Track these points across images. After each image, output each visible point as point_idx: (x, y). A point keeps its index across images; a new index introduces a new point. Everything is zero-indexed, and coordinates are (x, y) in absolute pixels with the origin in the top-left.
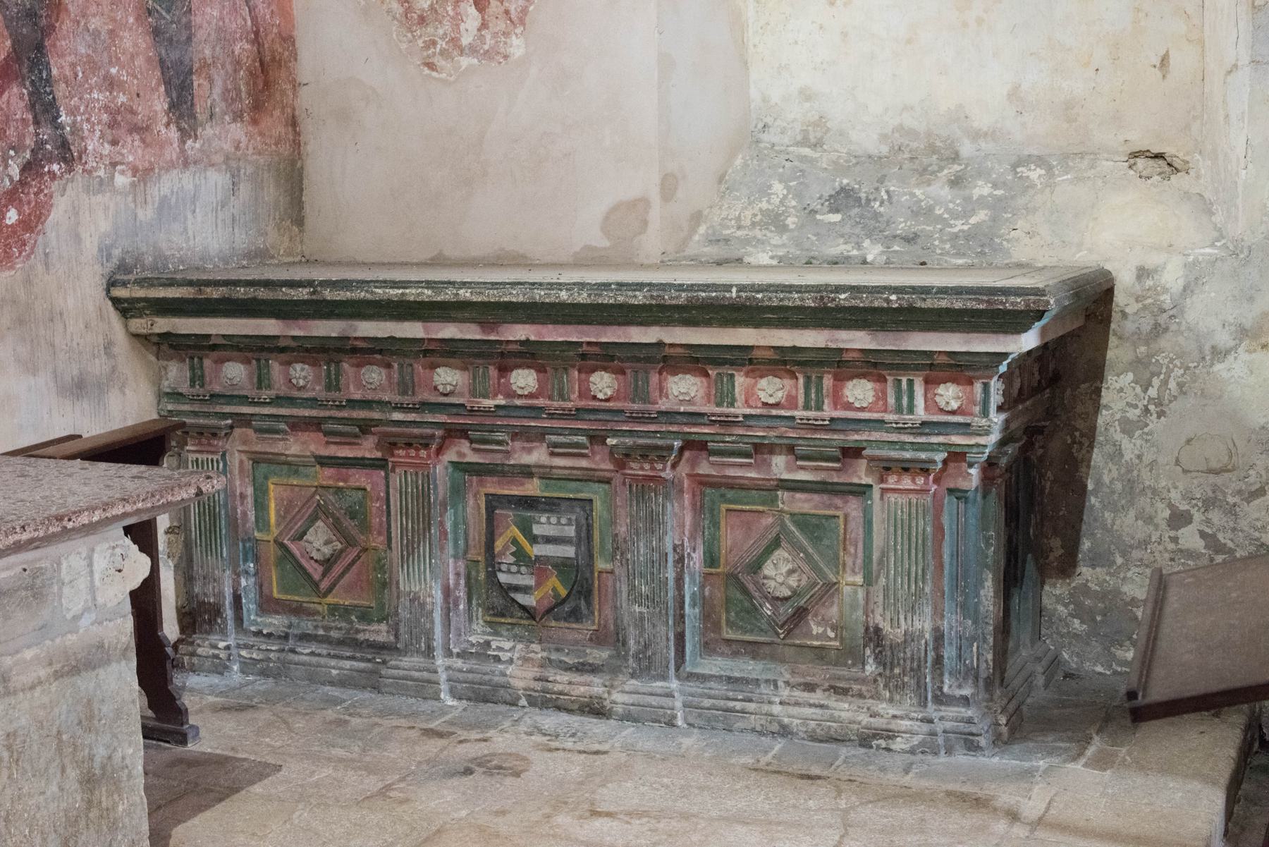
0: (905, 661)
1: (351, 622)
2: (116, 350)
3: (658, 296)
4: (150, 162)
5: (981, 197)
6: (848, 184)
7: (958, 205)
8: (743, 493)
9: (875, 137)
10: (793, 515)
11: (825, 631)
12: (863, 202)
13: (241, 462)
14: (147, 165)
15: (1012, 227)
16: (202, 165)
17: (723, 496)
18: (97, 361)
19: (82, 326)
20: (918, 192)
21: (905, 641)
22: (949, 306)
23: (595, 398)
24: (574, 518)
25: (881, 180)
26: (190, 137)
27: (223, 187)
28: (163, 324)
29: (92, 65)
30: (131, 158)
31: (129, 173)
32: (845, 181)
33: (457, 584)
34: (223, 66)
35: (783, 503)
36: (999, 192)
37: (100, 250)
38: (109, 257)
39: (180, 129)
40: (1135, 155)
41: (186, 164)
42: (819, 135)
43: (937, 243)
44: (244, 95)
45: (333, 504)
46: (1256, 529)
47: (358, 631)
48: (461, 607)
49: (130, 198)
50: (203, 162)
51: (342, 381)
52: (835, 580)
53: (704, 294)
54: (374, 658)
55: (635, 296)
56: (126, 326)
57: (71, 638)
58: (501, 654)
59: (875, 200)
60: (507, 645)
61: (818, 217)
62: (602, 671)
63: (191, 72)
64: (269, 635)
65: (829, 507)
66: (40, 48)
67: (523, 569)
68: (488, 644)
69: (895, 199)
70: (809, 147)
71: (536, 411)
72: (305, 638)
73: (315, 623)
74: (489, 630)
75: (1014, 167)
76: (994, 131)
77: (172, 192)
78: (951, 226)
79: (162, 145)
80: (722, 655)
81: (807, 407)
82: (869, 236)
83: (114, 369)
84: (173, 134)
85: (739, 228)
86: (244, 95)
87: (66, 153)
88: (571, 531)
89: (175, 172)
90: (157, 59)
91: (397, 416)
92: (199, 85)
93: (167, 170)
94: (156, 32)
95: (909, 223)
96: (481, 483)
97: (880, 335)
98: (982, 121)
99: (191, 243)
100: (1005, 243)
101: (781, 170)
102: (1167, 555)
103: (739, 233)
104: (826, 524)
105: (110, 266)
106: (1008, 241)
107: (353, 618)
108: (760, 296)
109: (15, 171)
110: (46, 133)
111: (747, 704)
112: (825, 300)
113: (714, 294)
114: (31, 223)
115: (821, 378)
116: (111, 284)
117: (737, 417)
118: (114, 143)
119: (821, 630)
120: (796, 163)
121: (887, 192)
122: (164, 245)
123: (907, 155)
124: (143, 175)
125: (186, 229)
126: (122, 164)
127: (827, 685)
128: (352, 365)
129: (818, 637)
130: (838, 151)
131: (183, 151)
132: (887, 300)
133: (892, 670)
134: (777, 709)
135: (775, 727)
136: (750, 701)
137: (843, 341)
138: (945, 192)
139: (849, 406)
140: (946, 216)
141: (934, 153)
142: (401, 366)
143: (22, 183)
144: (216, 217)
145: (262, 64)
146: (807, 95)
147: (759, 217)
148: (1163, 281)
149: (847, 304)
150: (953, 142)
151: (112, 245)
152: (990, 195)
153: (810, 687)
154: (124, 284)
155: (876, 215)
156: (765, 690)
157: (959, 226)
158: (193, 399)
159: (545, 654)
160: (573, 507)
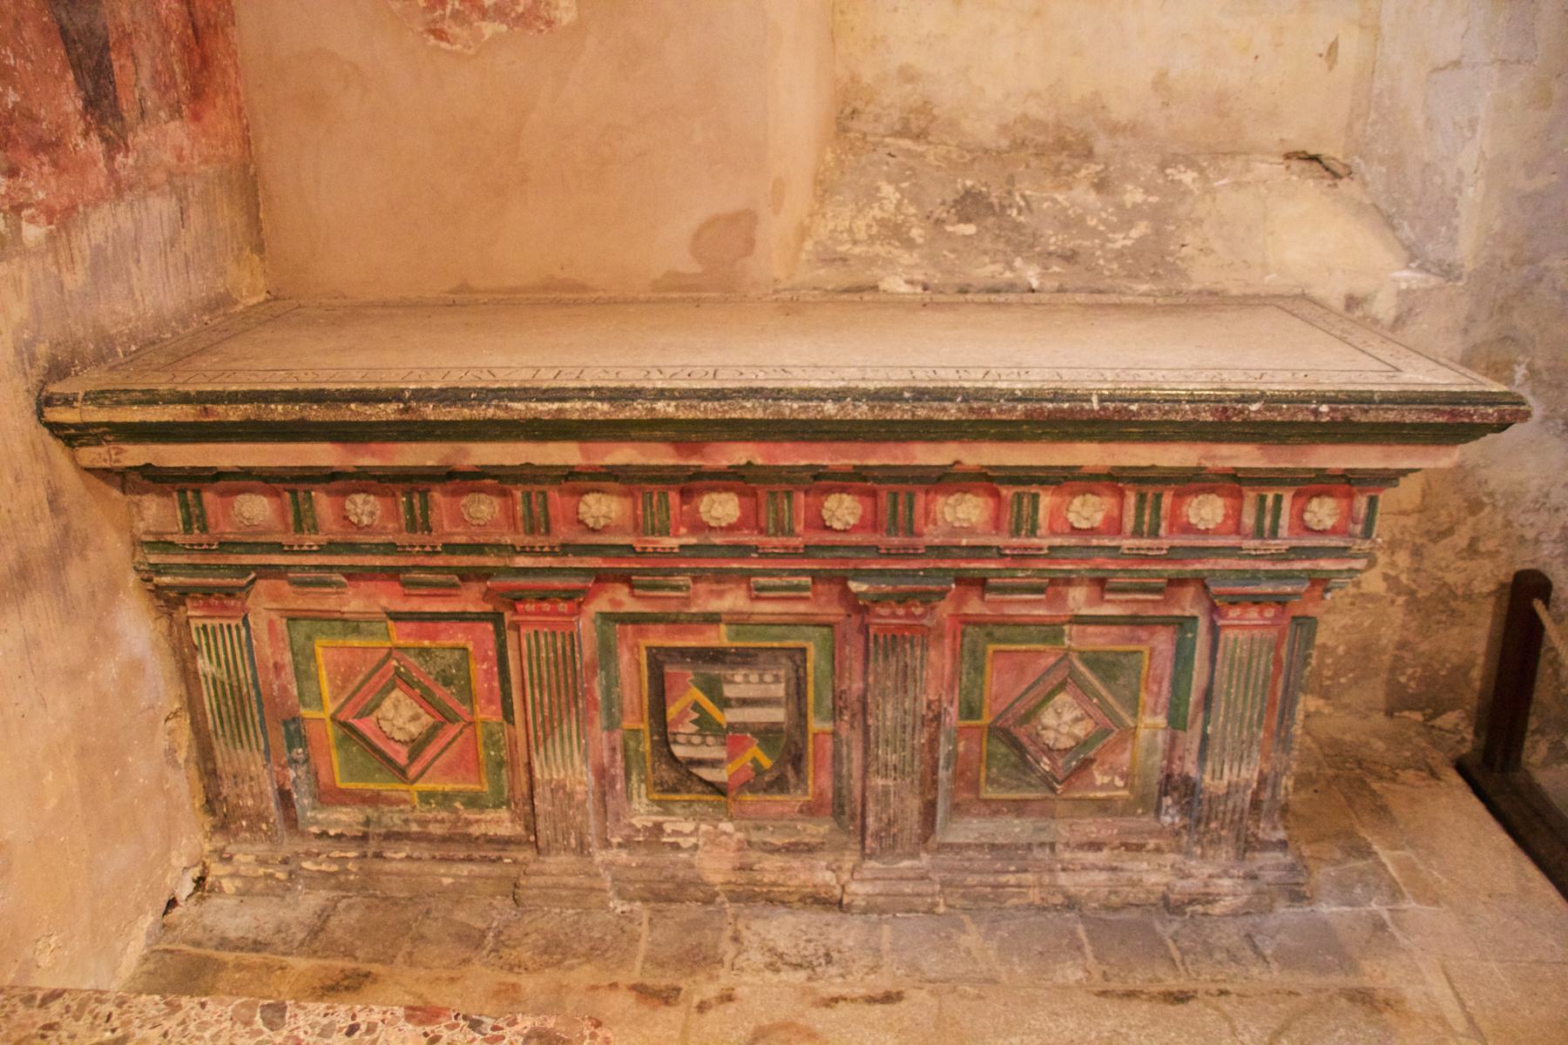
0: (1224, 813)
1: (456, 811)
2: (65, 500)
3: (981, 409)
4: (69, 196)
5: (1135, 206)
6: (973, 187)
7: (1112, 214)
8: (1018, 630)
9: (993, 127)
10: (1081, 653)
11: (1112, 781)
12: (997, 209)
13: (271, 624)
14: (65, 201)
15: (1181, 242)
16: (139, 191)
17: (990, 635)
18: (41, 526)
19: (10, 481)
20: (1060, 197)
21: (1228, 793)
22: (1398, 419)
23: (830, 529)
24: (782, 673)
25: (1011, 180)
26: (119, 149)
27: (170, 218)
28: (136, 454)
30: (41, 195)
31: (42, 219)
32: (969, 183)
33: (613, 761)
34: (149, 37)
35: (1070, 639)
36: (1153, 199)
37: (18, 352)
38: (33, 358)
39: (105, 139)
40: (1288, 156)
41: (119, 193)
42: (923, 124)
43: (1101, 262)
44: (179, 78)
45: (417, 670)
46: (1441, 569)
47: (469, 823)
48: (618, 787)
49: (50, 259)
51: (433, 517)
52: (1132, 725)
53: (1050, 406)
54: (500, 858)
55: (944, 409)
56: (74, 459)
58: (680, 840)
59: (1010, 206)
60: (688, 827)
61: (949, 228)
62: (822, 850)
63: (106, 48)
64: (339, 837)
65: (1130, 640)
67: (710, 740)
68: (658, 828)
69: (1034, 206)
70: (911, 138)
71: (742, 551)
72: (393, 836)
73: (403, 817)
74: (656, 808)
75: (1162, 167)
76: (1135, 126)
77: (107, 237)
78: (1110, 241)
79: (84, 165)
80: (978, 815)
81: (1138, 533)
82: (1018, 252)
83: (66, 529)
84: (97, 147)
85: (855, 242)
86: (179, 78)
88: (779, 690)
89: (107, 206)
90: (57, 27)
91: (522, 561)
92: (121, 67)
93: (96, 206)
95: (1060, 237)
96: (641, 634)
97: (1275, 450)
98: (1121, 111)
99: (141, 308)
100: (1178, 262)
101: (885, 168)
102: (1348, 600)
103: (857, 250)
104: (1125, 662)
105: (35, 375)
106: (1182, 260)
107: (458, 805)
108: (1134, 407)
111: (1023, 876)
112: (1230, 413)
113: (1066, 405)
115: (1158, 497)
116: (45, 402)
117: (1040, 549)
119: (1106, 779)
120: (901, 159)
121: (1023, 196)
122: (106, 321)
123: (1031, 150)
124: (63, 218)
125: (131, 291)
126: (29, 206)
127: (1117, 843)
128: (445, 493)
129: (1102, 788)
130: (945, 144)
131: (112, 172)
132: (1316, 412)
133: (1207, 824)
134: (1063, 879)
135: (1058, 899)
136: (1025, 871)
137: (1222, 458)
138: (1092, 198)
139: (1189, 529)
140: (1102, 228)
141: (1063, 149)
142: (528, 495)
144: (166, 263)
145: (195, 30)
146: (907, 75)
147: (875, 230)
148: (1374, 311)
149: (1259, 418)
150: (1086, 137)
151: (35, 339)
152: (1145, 202)
153: (1096, 846)
154: (68, 402)
155: (1018, 227)
156: (1043, 855)
157: (1120, 241)
158: (190, 549)
159: (740, 835)
160: (776, 659)
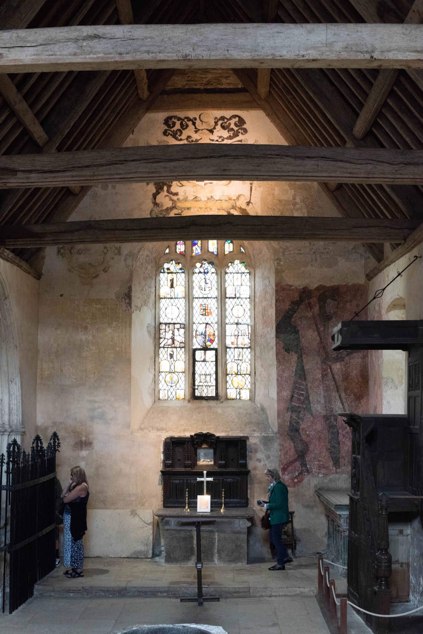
29: (315, 458)
37: (315, 486)
38: (317, 487)
39: (335, 467)
41: (337, 473)
50: (343, 472)
57: (235, 529)
63: (339, 458)
66: (304, 456)
84: (334, 468)
87: (308, 471)
94: (331, 453)
105: (316, 489)
109: (297, 474)
110: (304, 468)
114: (300, 481)
118: (319, 470)
124: (326, 475)
131: (336, 471)
143: (298, 476)
